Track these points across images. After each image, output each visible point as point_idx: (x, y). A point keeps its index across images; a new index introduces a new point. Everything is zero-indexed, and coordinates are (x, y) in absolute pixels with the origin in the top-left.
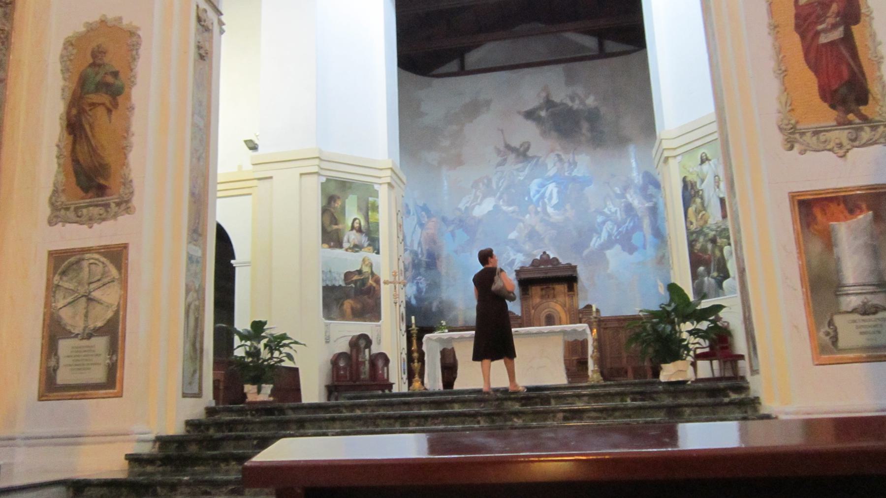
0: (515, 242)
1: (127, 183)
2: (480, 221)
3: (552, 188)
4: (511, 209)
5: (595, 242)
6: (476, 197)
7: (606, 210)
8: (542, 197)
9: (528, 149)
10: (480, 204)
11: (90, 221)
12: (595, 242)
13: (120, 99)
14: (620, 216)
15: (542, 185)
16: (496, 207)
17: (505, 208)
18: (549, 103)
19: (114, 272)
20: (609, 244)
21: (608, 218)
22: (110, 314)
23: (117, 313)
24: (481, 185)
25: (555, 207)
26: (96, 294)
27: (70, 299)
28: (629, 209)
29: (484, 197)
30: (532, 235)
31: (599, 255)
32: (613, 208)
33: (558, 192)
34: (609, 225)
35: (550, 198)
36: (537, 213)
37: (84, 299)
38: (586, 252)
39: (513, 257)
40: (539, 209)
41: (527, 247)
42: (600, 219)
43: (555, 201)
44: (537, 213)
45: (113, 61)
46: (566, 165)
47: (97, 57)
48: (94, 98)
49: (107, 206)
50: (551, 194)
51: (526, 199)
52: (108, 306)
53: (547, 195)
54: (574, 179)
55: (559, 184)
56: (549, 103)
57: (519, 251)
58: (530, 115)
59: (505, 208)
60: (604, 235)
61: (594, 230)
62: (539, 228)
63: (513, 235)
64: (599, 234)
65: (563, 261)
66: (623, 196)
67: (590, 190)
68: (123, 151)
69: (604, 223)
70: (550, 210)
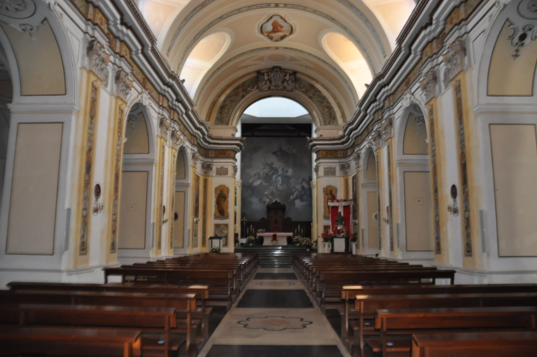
0: (266, 195)
1: (228, 214)
2: (255, 187)
3: (280, 178)
4: (266, 184)
5: (292, 197)
6: (255, 179)
7: (296, 188)
8: (276, 181)
9: (273, 165)
10: (256, 181)
11: (222, 219)
12: (292, 197)
13: (226, 200)
14: (300, 189)
15: (277, 177)
16: (261, 184)
17: (264, 184)
18: (281, 150)
19: (226, 228)
20: (296, 198)
21: (296, 190)
22: (225, 235)
23: (227, 234)
24: (256, 175)
25: (281, 185)
26: (223, 231)
27: (218, 232)
28: (303, 188)
29: (258, 179)
30: (272, 194)
31: (293, 203)
32: (298, 187)
33: (282, 180)
34: (296, 192)
35: (279, 182)
36: (274, 186)
37: (221, 232)
38: (289, 200)
39: (265, 200)
40: (275, 185)
41: (270, 197)
42: (294, 190)
43: (280, 183)
44: (274, 186)
45: (225, 193)
46: (285, 172)
47: (222, 191)
48: (221, 199)
49: (224, 217)
50: (279, 180)
51: (271, 181)
52: (225, 233)
53: (278, 181)
54: (287, 176)
55: (282, 178)
56: (281, 150)
57: (268, 198)
58: (275, 153)
59: (264, 184)
60: (295, 195)
61: (292, 194)
62: (275, 191)
63: (266, 193)
64: (293, 195)
65: (282, 203)
66: (301, 183)
67: (292, 180)
68: (227, 208)
69: (295, 191)
70: (279, 186)
